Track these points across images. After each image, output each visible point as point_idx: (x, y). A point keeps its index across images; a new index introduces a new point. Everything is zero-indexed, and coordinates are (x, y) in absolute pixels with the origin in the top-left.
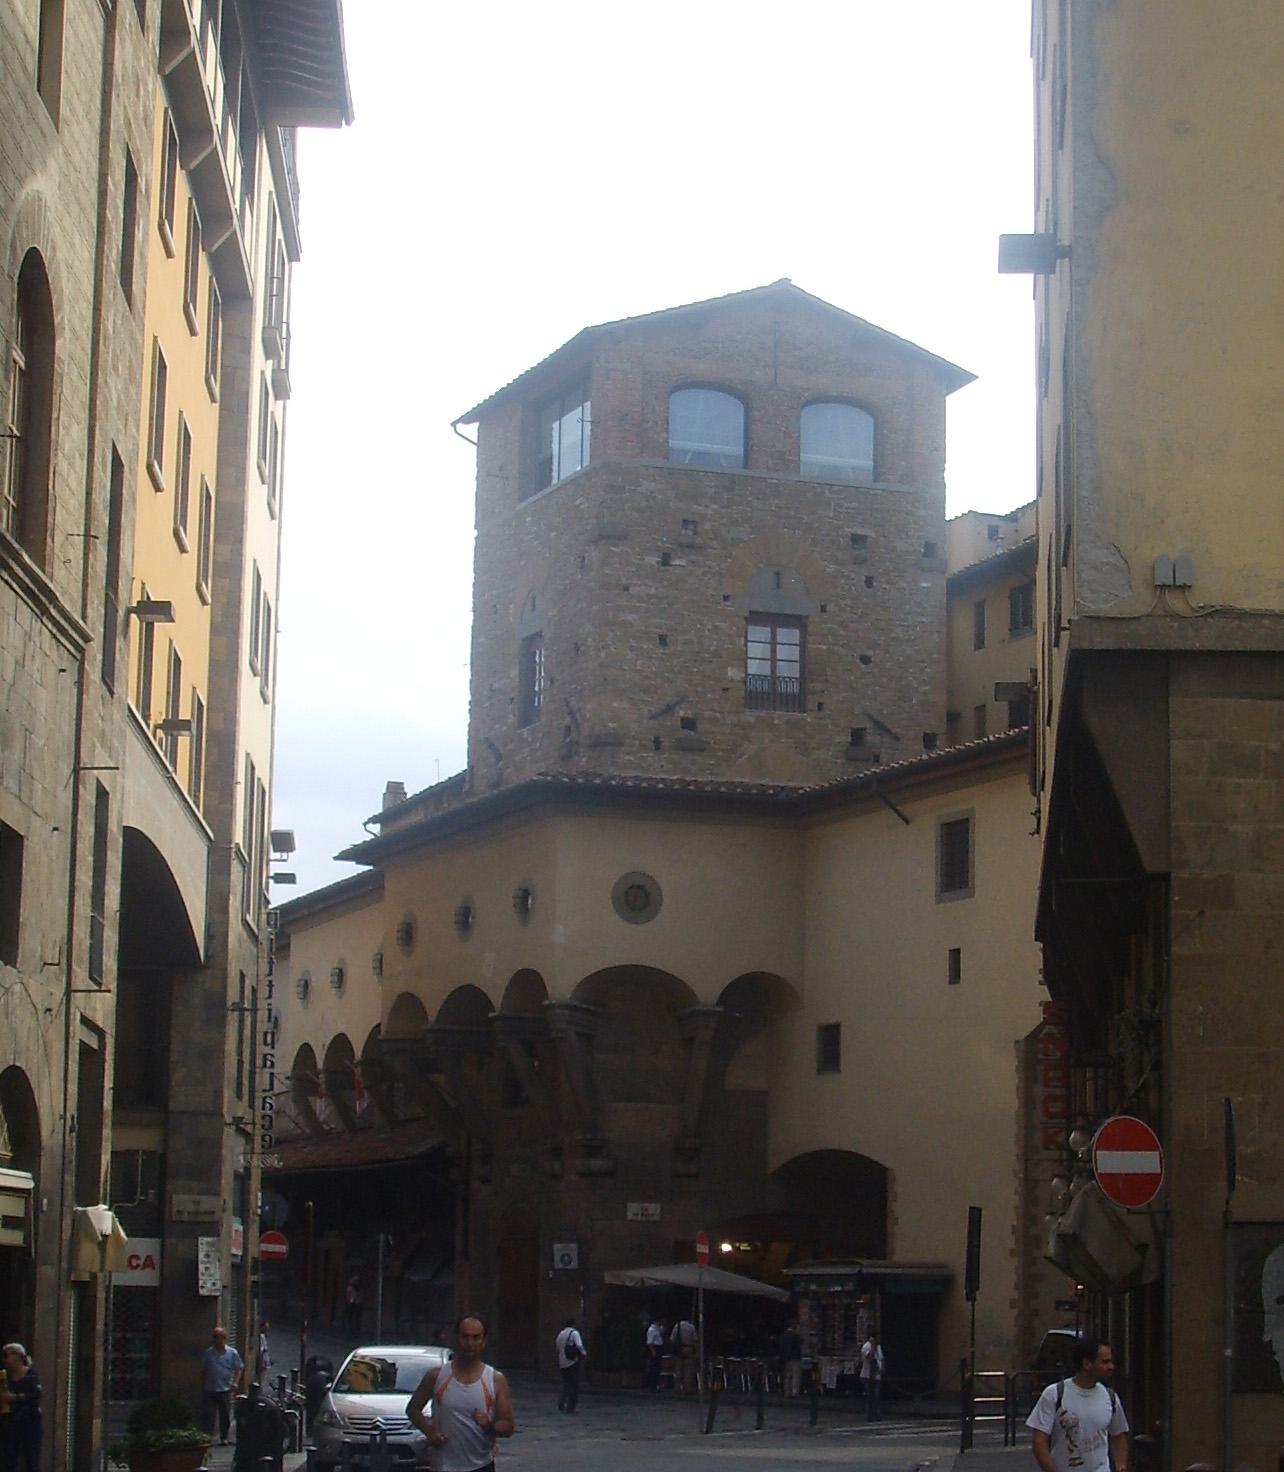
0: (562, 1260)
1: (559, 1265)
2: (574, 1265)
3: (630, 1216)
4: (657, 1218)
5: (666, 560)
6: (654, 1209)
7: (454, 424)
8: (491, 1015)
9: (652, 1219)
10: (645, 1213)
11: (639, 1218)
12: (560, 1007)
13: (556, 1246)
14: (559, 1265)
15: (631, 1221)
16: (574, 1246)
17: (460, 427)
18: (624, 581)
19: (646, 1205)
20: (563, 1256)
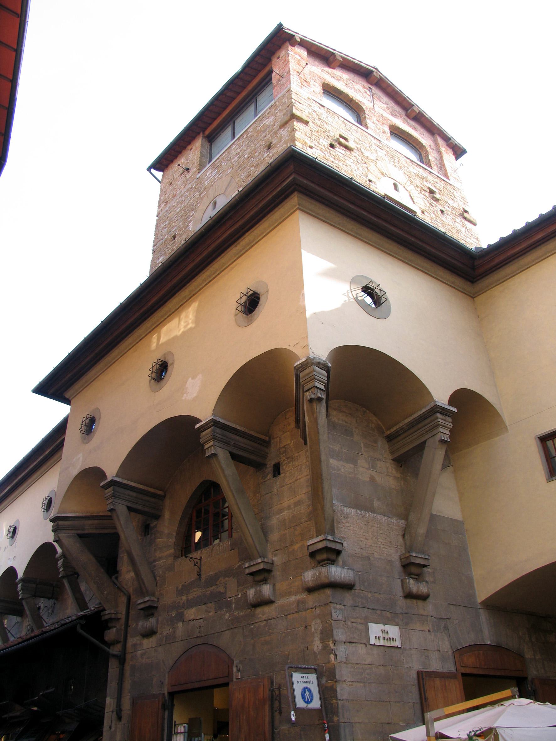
0: (303, 696)
1: (300, 704)
2: (316, 704)
3: (373, 641)
4: (397, 643)
5: (332, 146)
6: (394, 631)
7: (149, 169)
8: (197, 426)
9: (393, 644)
10: (386, 636)
11: (382, 643)
12: (319, 364)
13: (296, 677)
14: (300, 704)
15: (375, 645)
16: (313, 677)
17: (153, 171)
18: (309, 143)
19: (387, 627)
20: (305, 689)
